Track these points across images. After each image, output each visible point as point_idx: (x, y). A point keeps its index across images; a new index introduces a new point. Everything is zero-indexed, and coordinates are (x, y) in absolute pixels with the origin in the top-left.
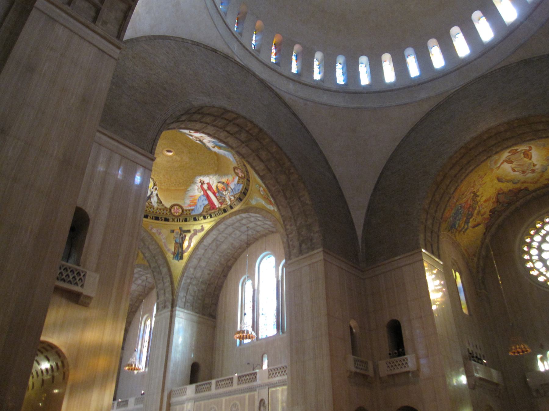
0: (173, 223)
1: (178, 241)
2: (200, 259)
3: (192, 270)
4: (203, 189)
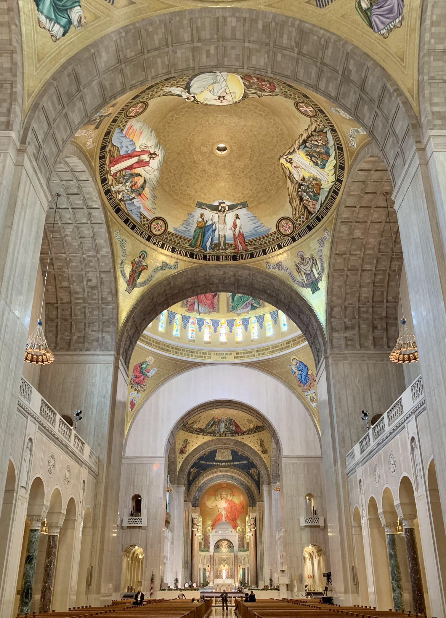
4: (143, 152)
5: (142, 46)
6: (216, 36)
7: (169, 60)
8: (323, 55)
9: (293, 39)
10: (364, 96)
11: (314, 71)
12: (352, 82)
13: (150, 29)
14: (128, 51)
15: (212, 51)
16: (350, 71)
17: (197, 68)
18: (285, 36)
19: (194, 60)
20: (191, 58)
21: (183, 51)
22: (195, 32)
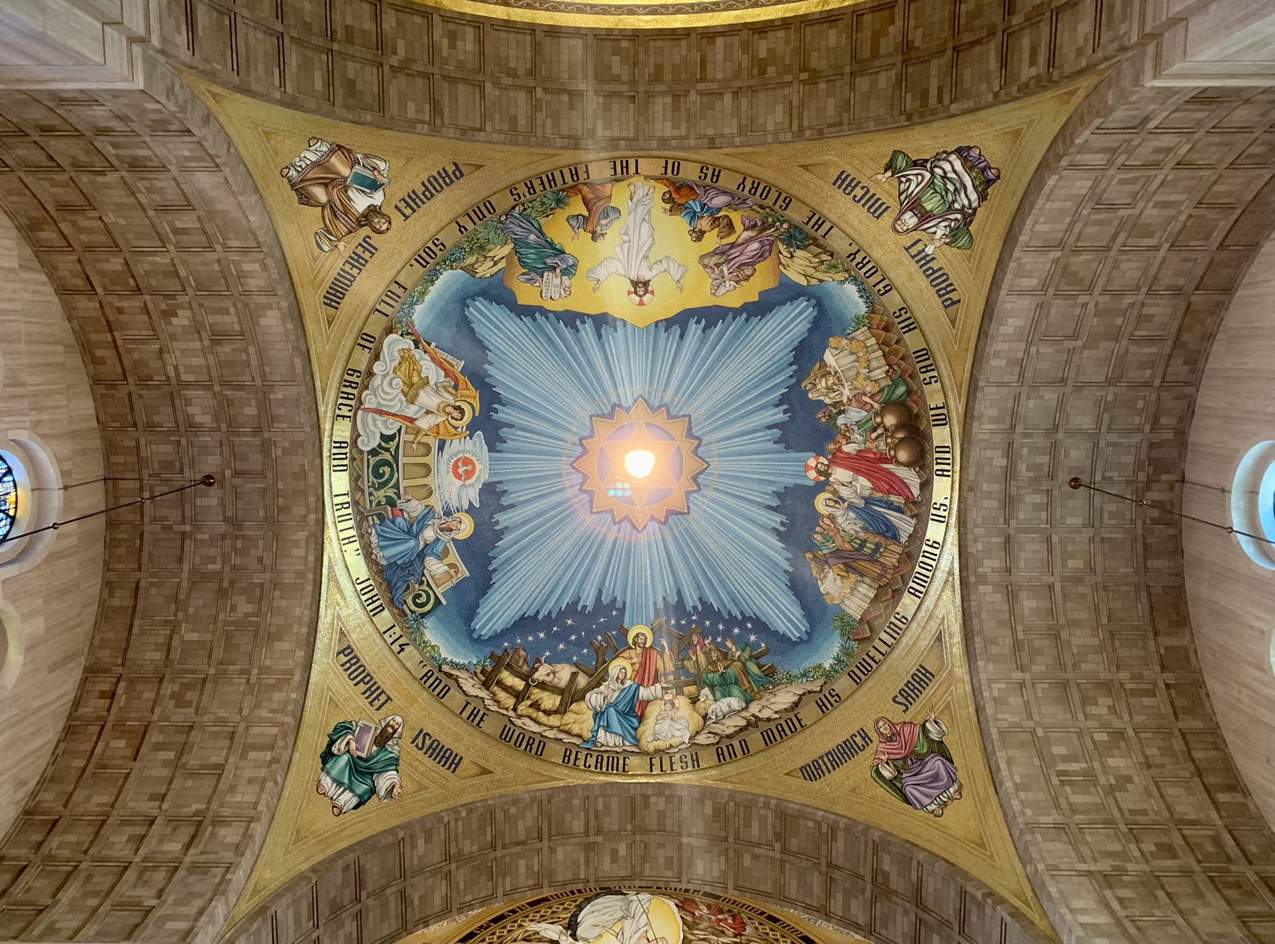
5: (494, 837)
6: (629, 827)
7: (541, 864)
8: (830, 850)
9: (769, 828)
10: (925, 916)
11: (816, 882)
12: (896, 893)
13: (513, 810)
14: (468, 842)
15: (622, 851)
16: (886, 875)
17: (592, 880)
18: (755, 824)
19: (587, 865)
20: (582, 862)
21: (569, 848)
22: (592, 818)
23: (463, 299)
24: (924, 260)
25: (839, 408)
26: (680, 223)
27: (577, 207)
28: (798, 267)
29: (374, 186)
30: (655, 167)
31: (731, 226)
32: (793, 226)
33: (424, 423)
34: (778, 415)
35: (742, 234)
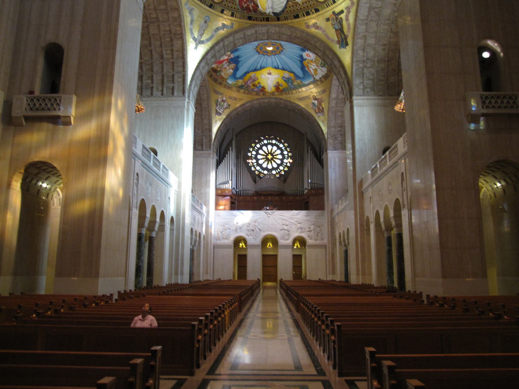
0: (325, 10)
1: (337, 28)
2: (365, 36)
3: (360, 52)
23: (303, 78)
24: (221, 94)
25: (228, 65)
26: (262, 85)
27: (281, 88)
28: (240, 82)
29: (313, 104)
30: (267, 94)
31: (253, 85)
32: (242, 88)
33: (315, 64)
34: (239, 59)
35: (251, 85)
